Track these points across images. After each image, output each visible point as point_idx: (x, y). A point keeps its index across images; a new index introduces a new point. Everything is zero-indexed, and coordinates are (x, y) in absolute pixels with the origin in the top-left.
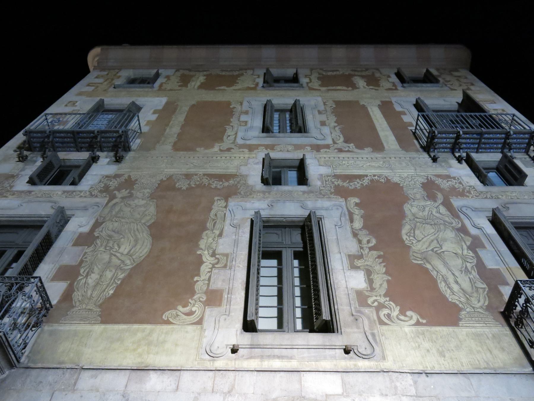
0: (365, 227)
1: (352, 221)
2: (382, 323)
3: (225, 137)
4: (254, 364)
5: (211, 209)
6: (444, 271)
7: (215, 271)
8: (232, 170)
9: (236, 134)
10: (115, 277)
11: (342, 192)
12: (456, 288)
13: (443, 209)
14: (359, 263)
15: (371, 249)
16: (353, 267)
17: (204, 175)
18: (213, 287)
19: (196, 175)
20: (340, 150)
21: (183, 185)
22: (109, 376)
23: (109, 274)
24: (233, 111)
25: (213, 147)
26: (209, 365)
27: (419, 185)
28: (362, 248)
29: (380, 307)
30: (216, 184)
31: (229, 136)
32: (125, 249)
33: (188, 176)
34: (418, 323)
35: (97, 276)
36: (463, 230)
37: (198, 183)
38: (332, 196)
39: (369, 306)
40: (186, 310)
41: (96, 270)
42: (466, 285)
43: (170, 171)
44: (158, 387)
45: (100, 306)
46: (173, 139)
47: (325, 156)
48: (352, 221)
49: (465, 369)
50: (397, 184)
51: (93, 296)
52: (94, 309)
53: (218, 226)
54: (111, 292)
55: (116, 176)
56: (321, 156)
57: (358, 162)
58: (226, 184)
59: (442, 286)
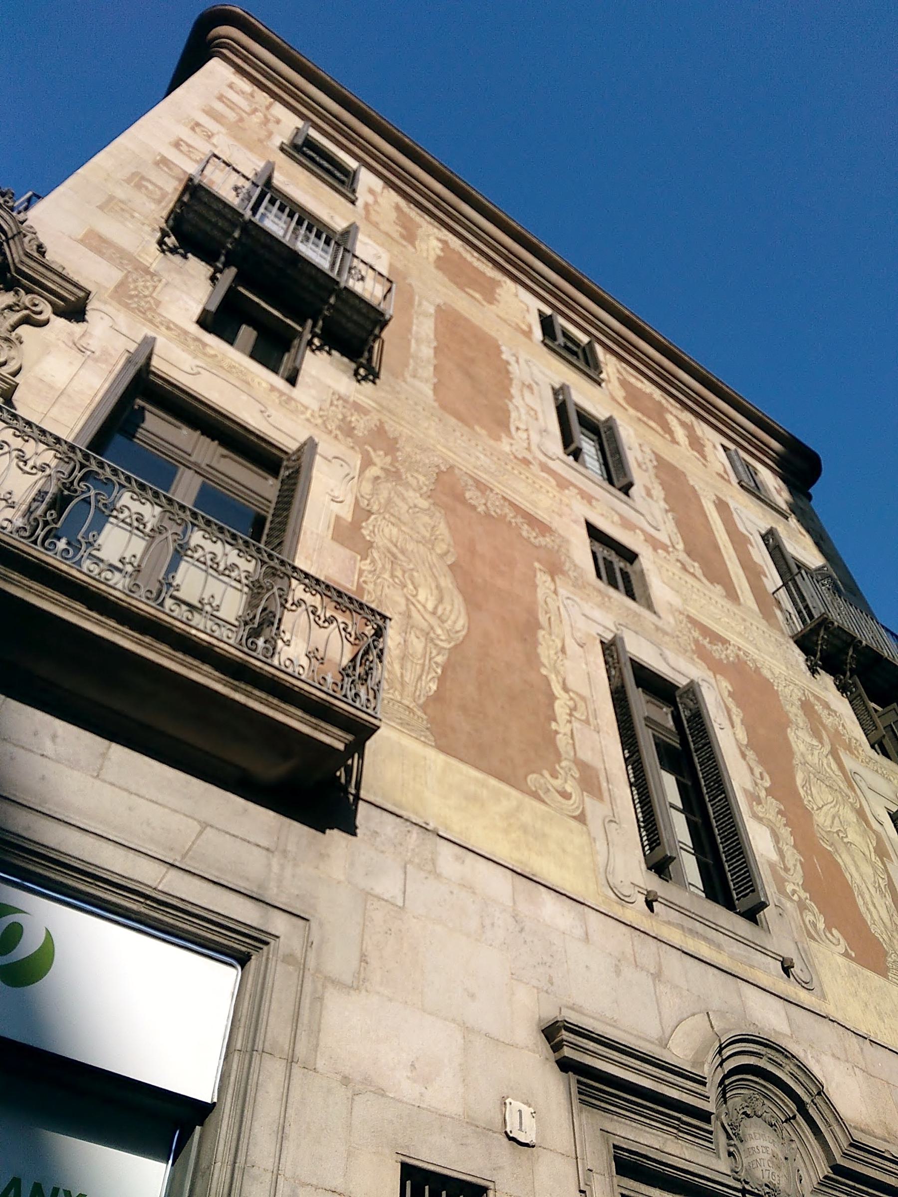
19: (492, 490)
23: (417, 645)
26: (617, 910)
33: (481, 486)
45: (424, 707)
51: (407, 679)
52: (415, 709)
54: (434, 687)
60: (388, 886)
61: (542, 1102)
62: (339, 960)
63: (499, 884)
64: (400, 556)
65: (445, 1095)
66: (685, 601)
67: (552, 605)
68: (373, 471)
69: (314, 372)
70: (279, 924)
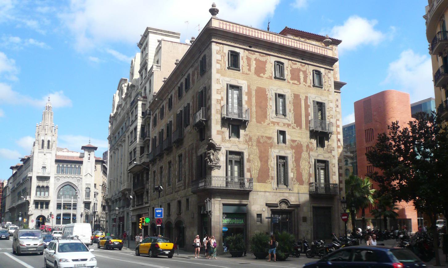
0: (295, 160)
1: (293, 158)
4: (279, 191)
5: (268, 152)
6: (304, 174)
8: (270, 136)
9: (270, 114)
10: (257, 172)
11: (292, 147)
12: (305, 177)
13: (308, 155)
14: (293, 171)
15: (295, 167)
16: (292, 172)
17: (266, 137)
20: (293, 128)
21: (261, 141)
23: (256, 171)
25: (265, 122)
27: (306, 146)
28: (293, 167)
29: (295, 181)
32: (256, 164)
33: (262, 137)
34: (298, 185)
36: (309, 163)
42: (306, 177)
44: (268, 194)
47: (290, 130)
48: (293, 158)
49: (302, 193)
50: (302, 145)
55: (247, 135)
58: (270, 142)
59: (303, 177)
60: (255, 197)
62: (252, 203)
63: (263, 193)
65: (259, 209)
66: (291, 137)
68: (250, 146)
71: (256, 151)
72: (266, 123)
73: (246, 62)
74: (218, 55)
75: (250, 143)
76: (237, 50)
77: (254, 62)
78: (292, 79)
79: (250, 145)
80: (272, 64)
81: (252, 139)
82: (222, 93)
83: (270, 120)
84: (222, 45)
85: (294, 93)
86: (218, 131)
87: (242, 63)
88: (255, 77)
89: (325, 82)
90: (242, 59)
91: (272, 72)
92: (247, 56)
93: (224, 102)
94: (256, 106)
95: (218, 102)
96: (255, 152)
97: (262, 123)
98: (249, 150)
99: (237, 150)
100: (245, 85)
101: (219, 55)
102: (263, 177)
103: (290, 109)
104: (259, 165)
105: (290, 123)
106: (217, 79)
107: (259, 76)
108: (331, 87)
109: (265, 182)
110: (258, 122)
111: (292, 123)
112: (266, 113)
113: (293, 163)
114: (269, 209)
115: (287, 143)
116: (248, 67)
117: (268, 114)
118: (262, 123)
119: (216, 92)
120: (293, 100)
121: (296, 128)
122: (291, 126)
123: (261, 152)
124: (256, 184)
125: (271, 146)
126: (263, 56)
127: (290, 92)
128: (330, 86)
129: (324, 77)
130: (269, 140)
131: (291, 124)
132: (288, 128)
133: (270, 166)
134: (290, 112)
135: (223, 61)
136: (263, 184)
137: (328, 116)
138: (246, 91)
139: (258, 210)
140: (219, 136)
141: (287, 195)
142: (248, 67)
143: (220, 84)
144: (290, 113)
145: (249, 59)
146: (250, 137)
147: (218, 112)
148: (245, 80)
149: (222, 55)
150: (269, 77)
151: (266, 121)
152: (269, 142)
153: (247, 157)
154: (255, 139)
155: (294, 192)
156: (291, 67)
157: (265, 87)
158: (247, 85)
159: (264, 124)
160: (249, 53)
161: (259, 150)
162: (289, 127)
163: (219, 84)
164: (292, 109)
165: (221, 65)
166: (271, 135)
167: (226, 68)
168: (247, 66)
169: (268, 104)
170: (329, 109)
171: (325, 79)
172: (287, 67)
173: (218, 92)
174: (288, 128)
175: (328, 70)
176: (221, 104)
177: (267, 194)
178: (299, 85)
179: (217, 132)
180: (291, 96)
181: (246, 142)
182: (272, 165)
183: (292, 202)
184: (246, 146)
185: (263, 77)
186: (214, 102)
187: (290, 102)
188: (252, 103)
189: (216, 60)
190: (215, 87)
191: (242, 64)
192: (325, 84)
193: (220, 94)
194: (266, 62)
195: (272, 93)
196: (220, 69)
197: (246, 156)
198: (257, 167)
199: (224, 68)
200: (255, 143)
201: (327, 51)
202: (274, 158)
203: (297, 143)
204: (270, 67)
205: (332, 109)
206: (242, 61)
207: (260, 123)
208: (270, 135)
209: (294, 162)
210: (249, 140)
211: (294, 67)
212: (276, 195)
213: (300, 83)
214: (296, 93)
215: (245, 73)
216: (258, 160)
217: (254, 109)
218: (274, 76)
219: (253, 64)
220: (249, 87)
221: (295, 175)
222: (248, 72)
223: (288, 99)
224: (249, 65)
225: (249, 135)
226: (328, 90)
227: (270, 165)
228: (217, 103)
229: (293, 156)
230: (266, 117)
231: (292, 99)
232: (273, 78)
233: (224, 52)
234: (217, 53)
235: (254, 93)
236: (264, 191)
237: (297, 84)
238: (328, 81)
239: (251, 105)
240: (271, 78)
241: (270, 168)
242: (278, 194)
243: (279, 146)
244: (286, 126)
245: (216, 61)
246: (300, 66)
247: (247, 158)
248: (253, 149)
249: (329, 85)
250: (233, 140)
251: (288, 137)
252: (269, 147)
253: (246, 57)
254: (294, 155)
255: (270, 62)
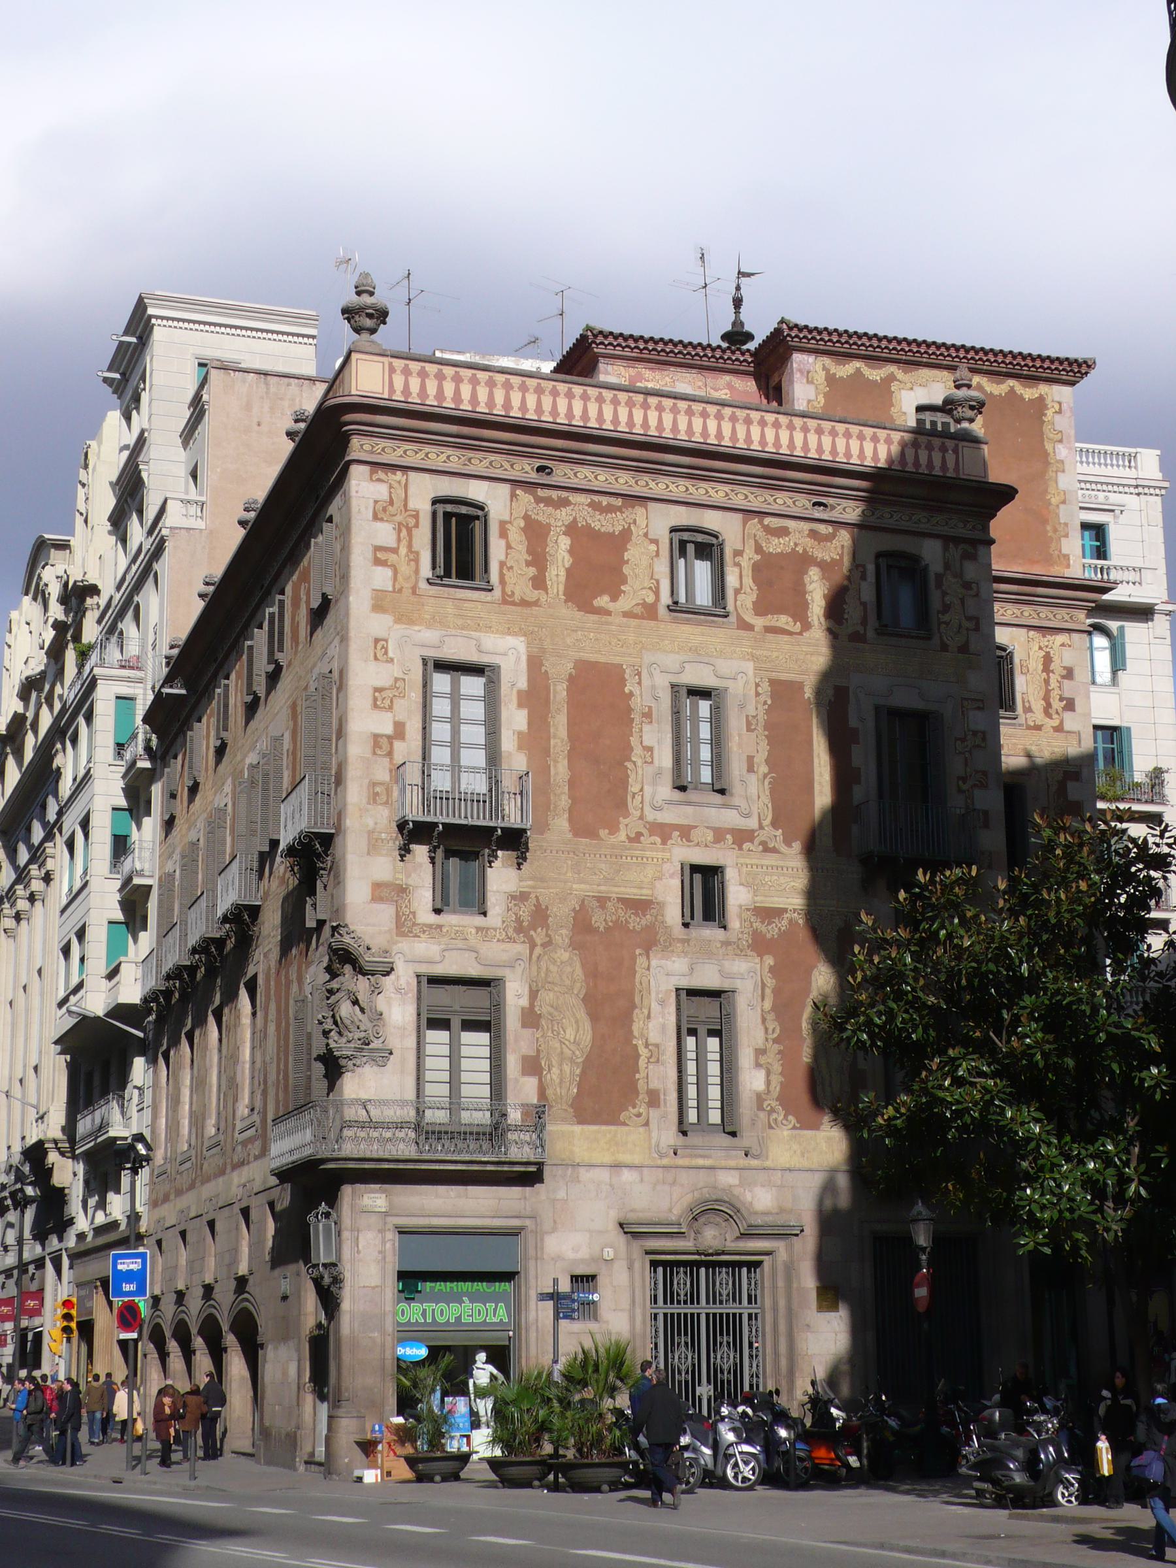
0: (774, 1008)
1: (763, 999)
2: (771, 1127)
3: (629, 799)
5: (635, 972)
7: (651, 1067)
8: (645, 894)
9: (641, 790)
11: (760, 945)
14: (762, 1060)
15: (775, 1041)
16: (758, 1065)
17: (619, 899)
18: (651, 1086)
20: (767, 849)
21: (599, 920)
22: (597, 1170)
23: (567, 1068)
24: (630, 710)
25: (618, 830)
26: (659, 1162)
28: (767, 1040)
29: (773, 1110)
30: (636, 922)
31: (634, 794)
32: (570, 1034)
33: (602, 901)
34: (794, 1128)
35: (558, 1072)
37: (614, 918)
38: (749, 953)
39: (764, 1110)
40: (635, 1111)
41: (554, 1063)
43: (581, 889)
45: (572, 1106)
46: (564, 801)
47: (748, 861)
48: (763, 999)
49: (813, 1167)
53: (645, 1002)
55: (522, 897)
56: (742, 860)
57: (782, 880)
58: (644, 922)
60: (561, 1194)
61: (615, 1246)
62: (547, 1225)
63: (604, 1175)
64: (556, 1013)
65: (584, 1253)
67: (644, 980)
68: (538, 950)
69: (495, 889)
70: (528, 1222)
71: (569, 969)
72: (622, 836)
73: (523, 548)
74: (379, 524)
75: (539, 936)
76: (476, 491)
77: (565, 542)
78: (761, 608)
79: (538, 941)
80: (655, 542)
81: (547, 917)
82: (399, 704)
83: (641, 818)
84: (399, 473)
85: (774, 675)
86: (377, 886)
87: (502, 552)
88: (569, 614)
89: (946, 608)
90: (503, 534)
91: (658, 582)
92: (526, 517)
93: (408, 749)
94: (571, 756)
95: (381, 748)
96: (564, 977)
97: (603, 833)
98: (534, 968)
99: (473, 970)
100: (518, 659)
101: (386, 524)
102: (607, 1091)
103: (750, 759)
104: (586, 1036)
105: (753, 823)
106: (377, 641)
107: (586, 607)
108: (977, 629)
109: (614, 1121)
110: (582, 829)
111: (761, 827)
112: (624, 783)
113: (764, 1020)
114: (638, 1246)
115: (734, 922)
116: (532, 571)
117: (634, 788)
118: (603, 833)
119: (370, 701)
120: (767, 712)
121: (783, 848)
122: (756, 842)
123: (592, 973)
124: (566, 1128)
125: (650, 941)
126: (610, 509)
127: (751, 673)
128: (971, 625)
129: (939, 585)
130: (636, 914)
131: (753, 831)
132: (741, 849)
133: (640, 1043)
134: (751, 769)
135: (403, 550)
136: (604, 1128)
137: (959, 778)
138: (523, 684)
139: (579, 1255)
140: (382, 906)
141: (728, 1179)
142: (532, 571)
143: (392, 660)
144: (753, 779)
145: (536, 533)
146: (538, 906)
147: (377, 794)
148: (515, 634)
149: (400, 524)
150: (638, 610)
151: (622, 826)
152: (636, 922)
153: (524, 1002)
154: (561, 913)
155: (768, 1163)
156: (758, 549)
157: (616, 660)
158: (524, 658)
159: (613, 839)
160: (538, 500)
161: (583, 966)
162: (746, 846)
163: (387, 661)
164: (761, 758)
165: (395, 572)
166: (649, 892)
167: (423, 585)
168: (528, 564)
169: (634, 740)
170: (963, 740)
171: (944, 594)
172: (738, 553)
173: (380, 699)
174: (741, 849)
175: (962, 546)
176: (391, 759)
177: (627, 1176)
178: (800, 634)
179: (373, 890)
180: (757, 694)
181: (519, 929)
182: (654, 1037)
183: (756, 1213)
184: (521, 948)
185: (609, 613)
186: (356, 749)
187: (749, 724)
188: (552, 742)
189: (371, 548)
190: (364, 675)
191: (503, 558)
192: (946, 618)
193: (391, 707)
194: (626, 535)
195: (653, 687)
196: (391, 589)
197: (519, 996)
198: (573, 1047)
199: (408, 586)
200: (562, 936)
201: (956, 451)
202: (662, 1003)
203: (785, 922)
204: (645, 562)
205: (984, 739)
206: (503, 542)
207: (592, 834)
208: (645, 892)
209: (770, 1017)
210: (532, 921)
211: (776, 545)
212: (674, 1183)
213: (807, 626)
214: (783, 676)
215: (517, 598)
216: (582, 1014)
217: (560, 770)
218: (665, 599)
219: (561, 550)
220: (535, 664)
221: (776, 1080)
222: (532, 595)
223: (742, 707)
224: (538, 559)
225: (533, 896)
226: (964, 649)
227: (642, 1035)
228: (374, 753)
229: (764, 985)
230: (621, 806)
231: (762, 710)
232: (662, 611)
233: (411, 505)
234: (376, 517)
235: (560, 692)
236: (607, 1159)
237: (790, 633)
238: (962, 600)
239: (547, 752)
240: (650, 611)
241: (643, 1052)
242: (685, 1177)
243: (688, 941)
244: (731, 841)
245: (370, 555)
246: (809, 542)
247: (523, 1009)
248: (554, 962)
249: (969, 619)
250: (453, 922)
251: (737, 896)
252: (638, 951)
253: (522, 524)
254: (770, 982)
255: (646, 535)
